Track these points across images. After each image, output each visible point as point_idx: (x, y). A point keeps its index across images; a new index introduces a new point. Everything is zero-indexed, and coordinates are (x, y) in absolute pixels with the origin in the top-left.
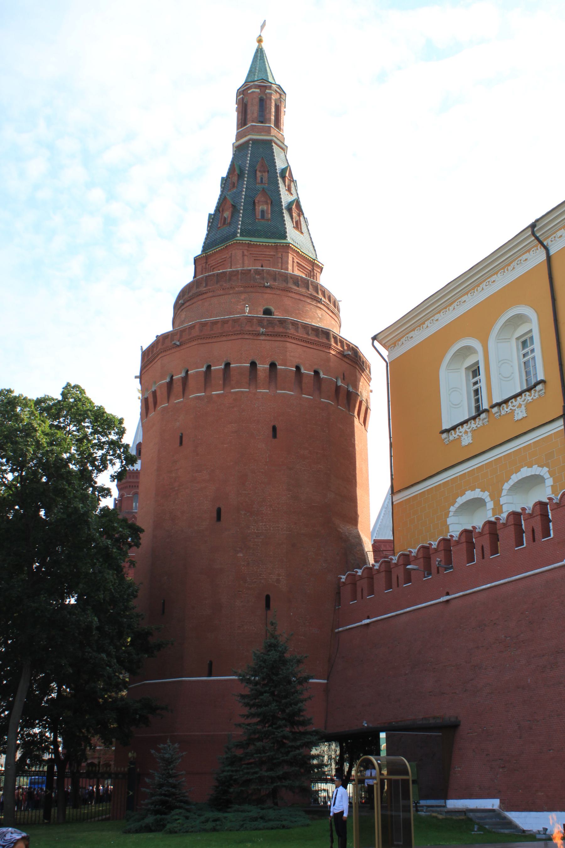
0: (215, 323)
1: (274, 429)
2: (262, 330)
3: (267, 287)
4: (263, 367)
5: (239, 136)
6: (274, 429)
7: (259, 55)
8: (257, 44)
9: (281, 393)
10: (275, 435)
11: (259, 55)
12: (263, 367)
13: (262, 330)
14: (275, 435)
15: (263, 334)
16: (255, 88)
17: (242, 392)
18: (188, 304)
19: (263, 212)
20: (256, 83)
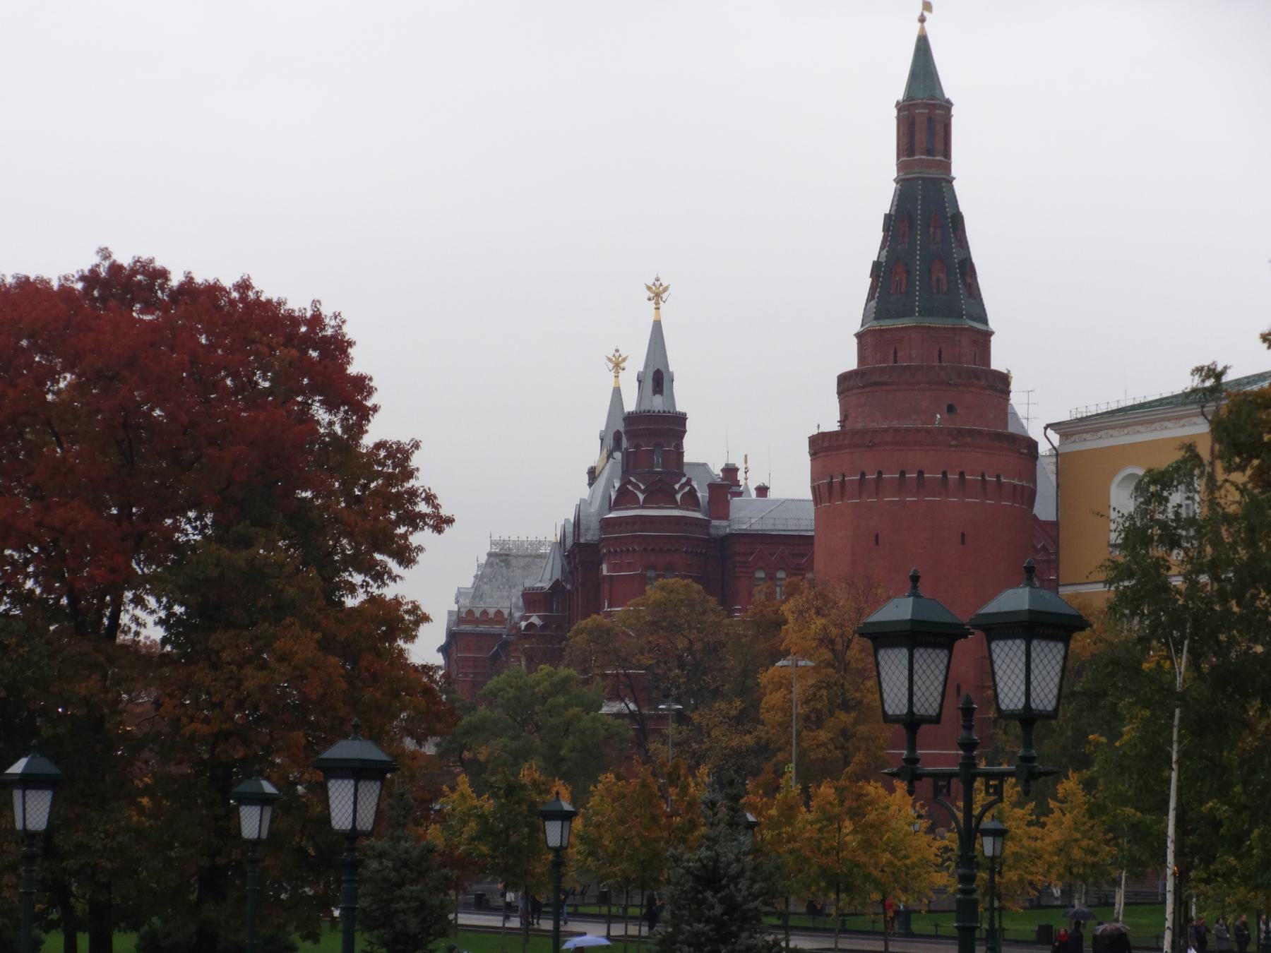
0: (908, 430)
1: (963, 535)
2: (953, 443)
3: (950, 384)
4: (953, 477)
5: (901, 167)
6: (963, 535)
7: (923, 48)
8: (919, 24)
9: (968, 502)
10: (963, 542)
11: (923, 48)
12: (953, 477)
13: (953, 443)
14: (963, 542)
15: (955, 446)
16: (923, 108)
17: (934, 501)
18: (868, 389)
19: (938, 279)
20: (924, 101)
